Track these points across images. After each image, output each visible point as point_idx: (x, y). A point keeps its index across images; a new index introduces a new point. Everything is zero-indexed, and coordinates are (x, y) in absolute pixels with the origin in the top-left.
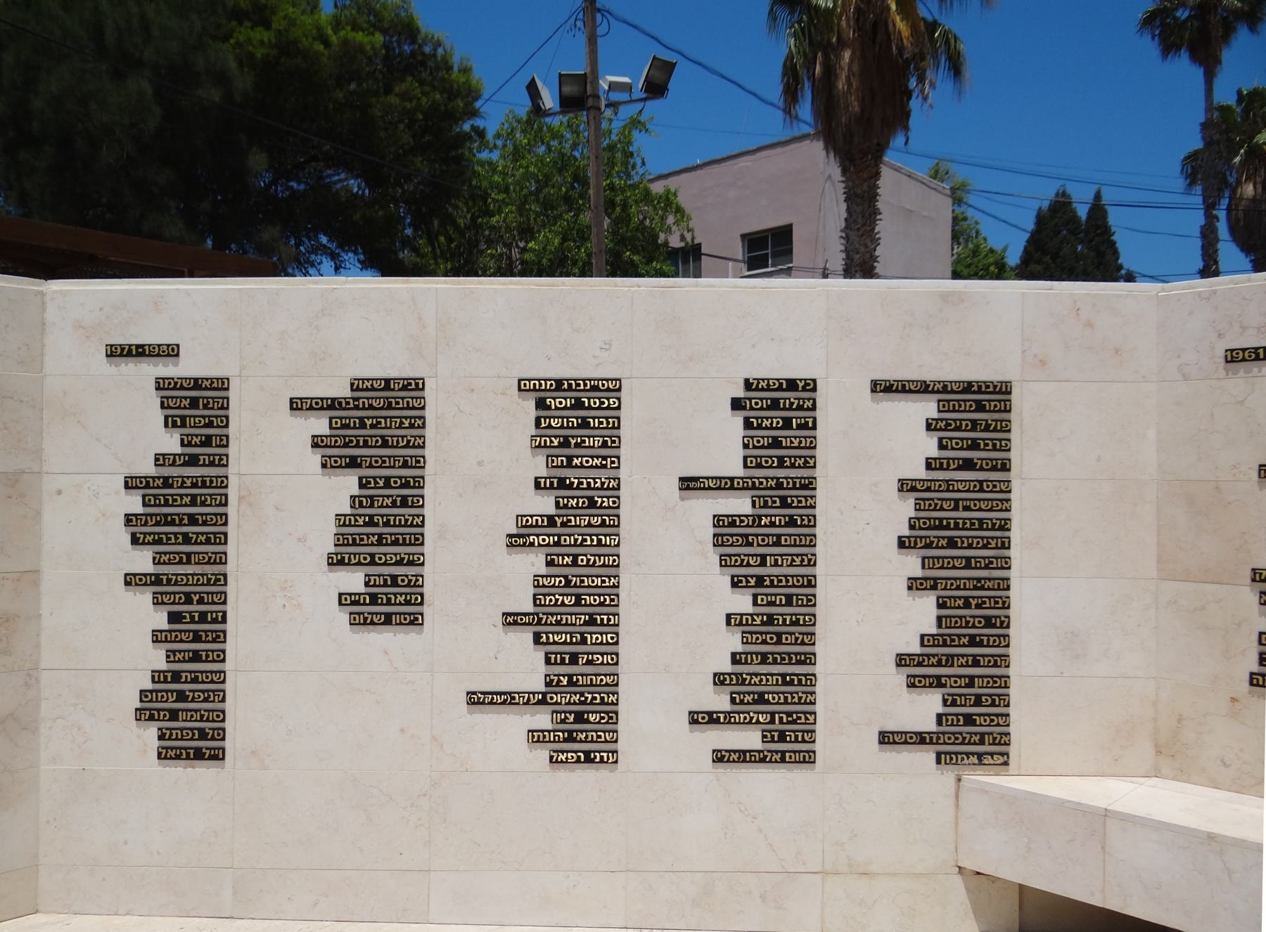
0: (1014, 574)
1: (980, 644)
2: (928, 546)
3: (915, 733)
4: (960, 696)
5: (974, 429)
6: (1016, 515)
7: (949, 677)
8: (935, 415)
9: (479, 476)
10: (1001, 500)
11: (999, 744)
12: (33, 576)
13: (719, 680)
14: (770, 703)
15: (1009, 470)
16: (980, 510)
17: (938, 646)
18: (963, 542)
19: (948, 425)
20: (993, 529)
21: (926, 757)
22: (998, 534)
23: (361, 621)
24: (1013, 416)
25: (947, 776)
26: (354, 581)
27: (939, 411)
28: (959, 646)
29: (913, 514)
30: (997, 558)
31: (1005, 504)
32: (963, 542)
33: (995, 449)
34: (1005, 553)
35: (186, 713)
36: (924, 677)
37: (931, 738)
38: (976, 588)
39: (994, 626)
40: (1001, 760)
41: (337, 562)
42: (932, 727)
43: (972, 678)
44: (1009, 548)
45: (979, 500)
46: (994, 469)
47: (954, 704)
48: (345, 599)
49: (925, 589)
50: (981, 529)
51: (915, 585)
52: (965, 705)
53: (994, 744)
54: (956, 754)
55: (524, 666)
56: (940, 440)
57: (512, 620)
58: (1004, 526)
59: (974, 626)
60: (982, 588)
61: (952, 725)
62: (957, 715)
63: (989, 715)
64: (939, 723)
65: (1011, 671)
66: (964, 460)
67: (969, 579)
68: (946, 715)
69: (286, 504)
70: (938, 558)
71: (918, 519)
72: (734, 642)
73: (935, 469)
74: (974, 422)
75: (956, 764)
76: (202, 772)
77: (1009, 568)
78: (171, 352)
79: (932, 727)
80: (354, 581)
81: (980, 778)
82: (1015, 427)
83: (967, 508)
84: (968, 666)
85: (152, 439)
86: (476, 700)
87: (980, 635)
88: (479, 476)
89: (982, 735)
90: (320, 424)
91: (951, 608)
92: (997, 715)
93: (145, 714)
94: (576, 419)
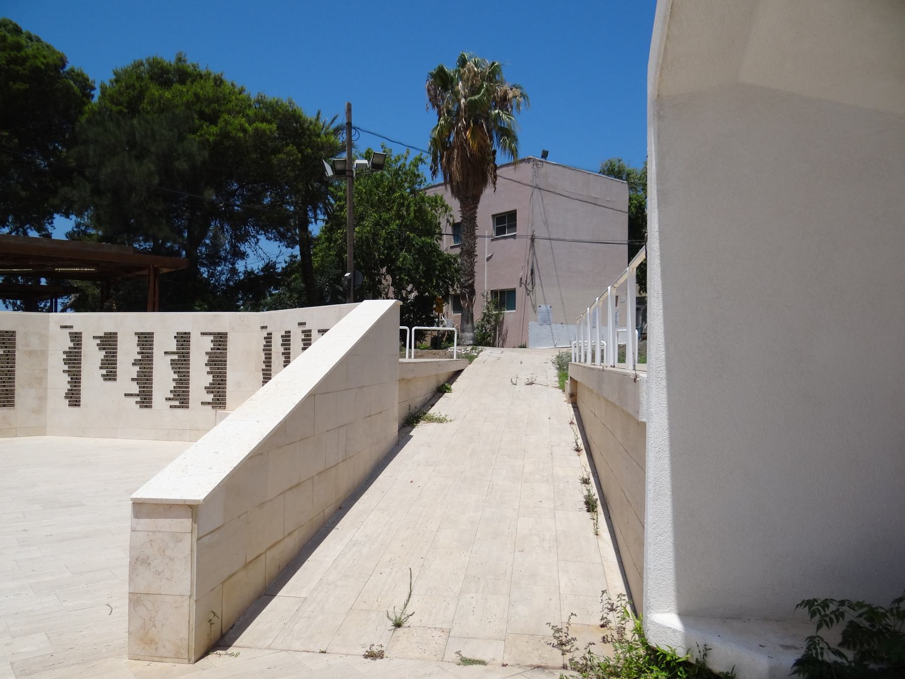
6: (228, 359)
9: (128, 351)
12: (47, 370)
13: (171, 391)
14: (181, 396)
21: (210, 407)
23: (105, 380)
25: (214, 411)
26: (104, 372)
31: (226, 357)
35: (74, 398)
41: (101, 368)
48: (103, 375)
51: (208, 373)
55: (135, 388)
57: (133, 380)
58: (225, 361)
69: (92, 356)
72: (174, 384)
76: (76, 408)
78: (71, 327)
80: (104, 372)
81: (220, 411)
85: (68, 344)
86: (126, 395)
88: (128, 351)
90: (98, 341)
93: (66, 397)
94: (145, 340)
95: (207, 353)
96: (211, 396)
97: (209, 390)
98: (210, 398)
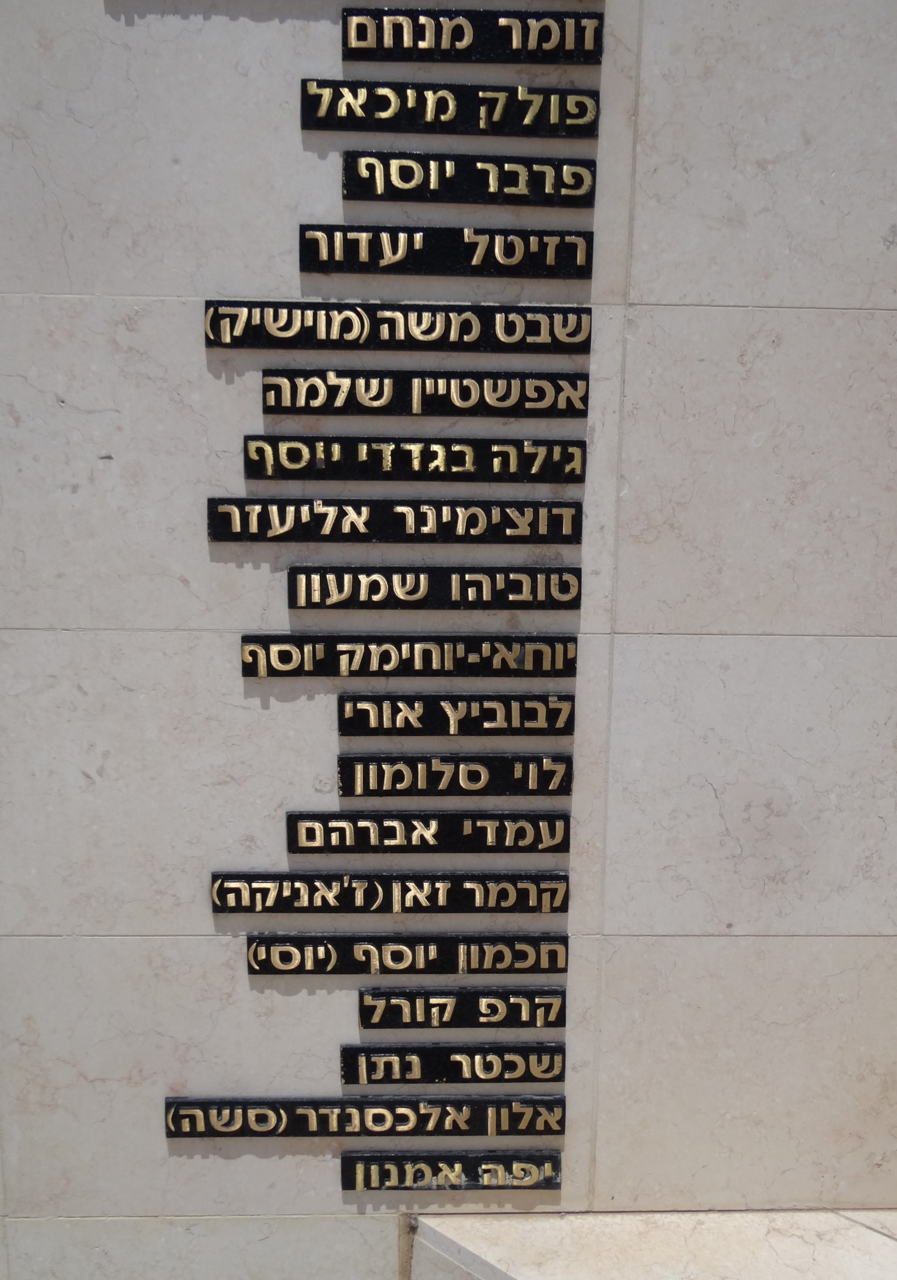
0: (590, 624)
1: (476, 843)
2: (307, 532)
3: (274, 1105)
4: (411, 996)
5: (465, 123)
6: (602, 430)
7: (379, 941)
8: (334, 67)
10: (553, 378)
11: (531, 1130)
15: (585, 272)
16: (482, 409)
17: (342, 848)
18: (421, 519)
19: (376, 103)
20: (523, 476)
22: (543, 492)
24: (610, 76)
25: (376, 1222)
27: (350, 54)
28: (407, 848)
29: (258, 424)
30: (532, 572)
32: (421, 519)
33: (537, 197)
34: (565, 554)
36: (301, 942)
37: (323, 1120)
38: (462, 668)
39: (520, 788)
40: (536, 1175)
42: (330, 1084)
43: (448, 945)
44: (576, 538)
45: (479, 377)
46: (532, 267)
47: (392, 1018)
49: (299, 672)
50: (483, 474)
51: (264, 661)
52: (427, 1024)
53: (514, 1130)
54: (400, 1160)
56: (350, 159)
58: (563, 466)
59: (454, 789)
60: (484, 669)
61: (388, 1078)
62: (402, 1051)
63: (500, 1050)
64: (350, 1074)
65: (575, 923)
66: (430, 234)
67: (440, 640)
68: (370, 1051)
70: (339, 573)
71: (274, 441)
73: (330, 267)
74: (467, 96)
75: (401, 1186)
77: (575, 604)
79: (330, 1084)
82: (612, 124)
83: (436, 405)
84: (433, 907)
87: (476, 816)
89: (478, 1107)
91: (380, 731)
92: (524, 1051)
95: (236, 332)
96: (331, 1014)
97: (283, 919)
98: (304, 1035)
